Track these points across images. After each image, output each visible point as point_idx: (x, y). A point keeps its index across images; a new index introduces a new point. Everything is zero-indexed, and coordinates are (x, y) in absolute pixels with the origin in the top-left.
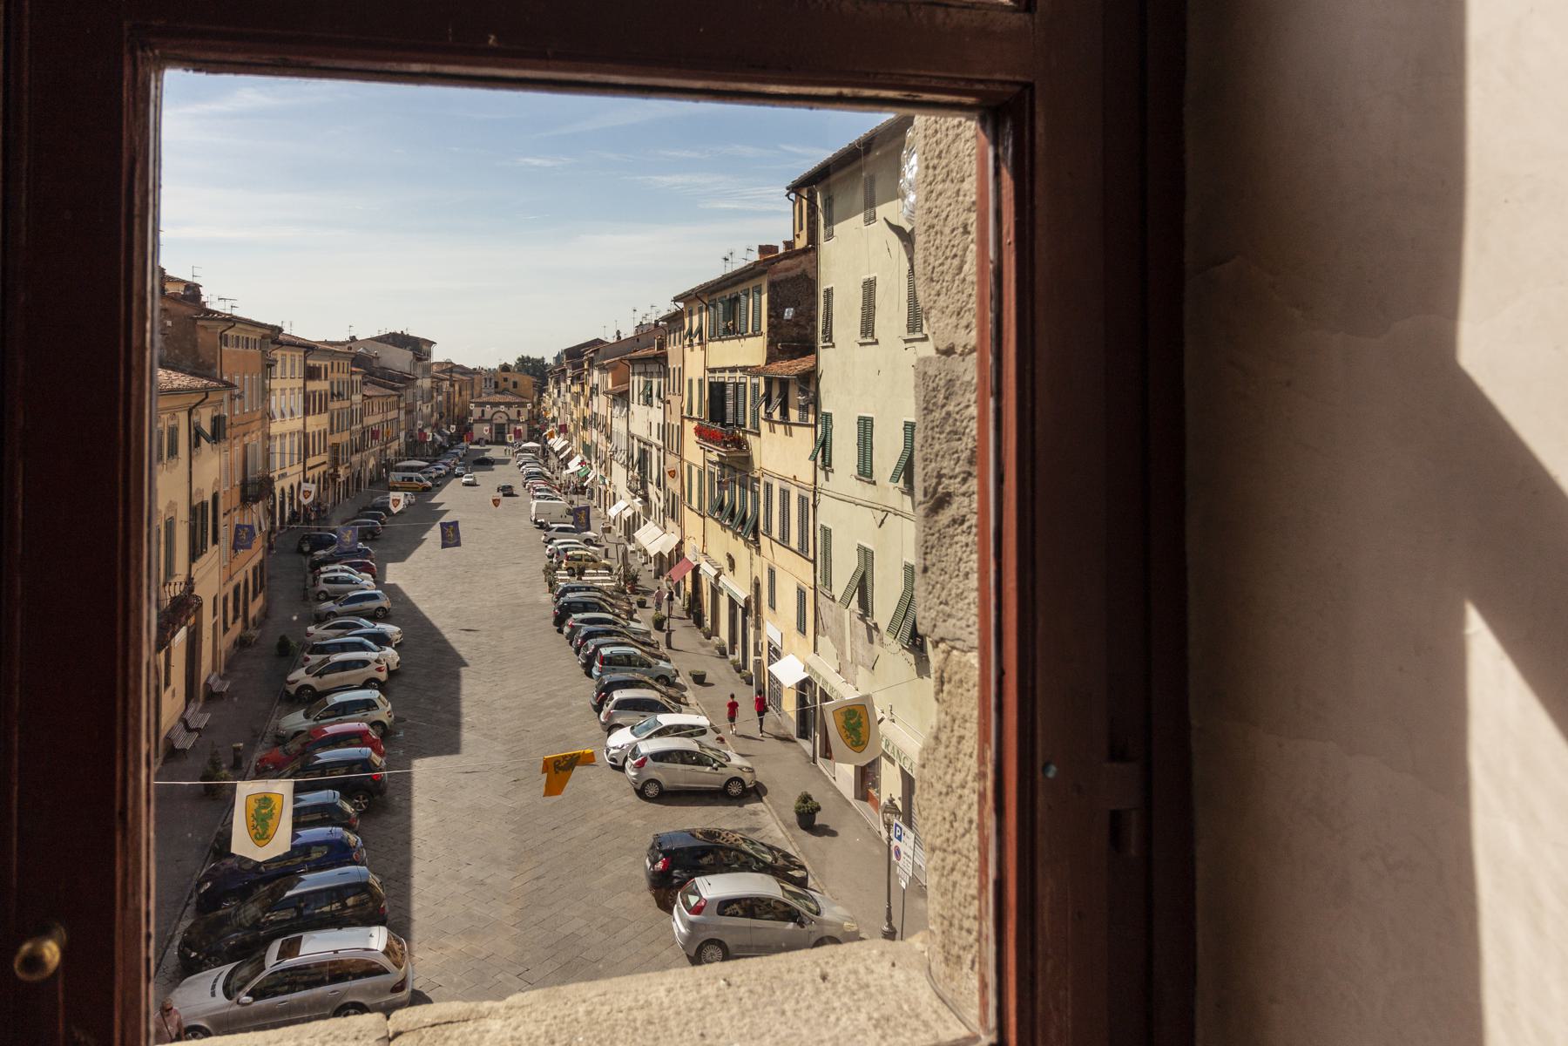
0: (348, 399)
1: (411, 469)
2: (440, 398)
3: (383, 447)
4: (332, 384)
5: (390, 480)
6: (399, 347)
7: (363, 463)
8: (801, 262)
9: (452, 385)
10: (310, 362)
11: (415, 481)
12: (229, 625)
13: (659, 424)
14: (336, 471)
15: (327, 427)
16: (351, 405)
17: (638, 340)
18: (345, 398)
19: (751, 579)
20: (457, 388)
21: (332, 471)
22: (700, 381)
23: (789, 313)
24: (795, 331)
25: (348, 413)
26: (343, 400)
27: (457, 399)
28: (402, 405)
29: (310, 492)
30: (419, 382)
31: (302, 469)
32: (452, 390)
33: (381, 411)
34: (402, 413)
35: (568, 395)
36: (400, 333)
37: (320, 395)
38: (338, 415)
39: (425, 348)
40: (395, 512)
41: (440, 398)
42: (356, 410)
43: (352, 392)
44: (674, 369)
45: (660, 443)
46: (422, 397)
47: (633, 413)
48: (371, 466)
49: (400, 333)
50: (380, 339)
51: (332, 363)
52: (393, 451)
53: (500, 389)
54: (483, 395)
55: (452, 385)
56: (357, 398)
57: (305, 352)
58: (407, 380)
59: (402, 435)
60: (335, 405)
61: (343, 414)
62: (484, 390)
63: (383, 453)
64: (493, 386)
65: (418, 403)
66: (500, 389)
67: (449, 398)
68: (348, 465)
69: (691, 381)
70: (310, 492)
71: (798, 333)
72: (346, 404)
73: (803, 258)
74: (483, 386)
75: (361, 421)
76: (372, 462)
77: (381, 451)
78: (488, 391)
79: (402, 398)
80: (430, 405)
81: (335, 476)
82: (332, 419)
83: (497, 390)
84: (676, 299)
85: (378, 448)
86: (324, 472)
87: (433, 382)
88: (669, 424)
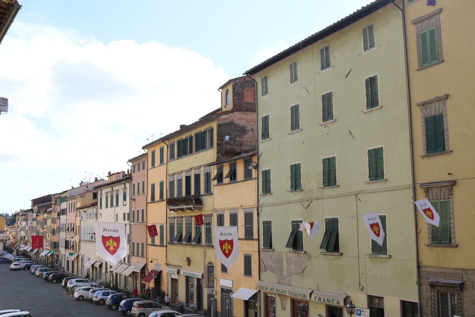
8: (231, 116)
13: (124, 214)
17: (87, 187)
19: (205, 264)
22: (162, 184)
23: (227, 138)
24: (228, 147)
35: (35, 224)
44: (139, 183)
45: (127, 222)
47: (101, 214)
69: (153, 186)
71: (230, 148)
73: (231, 114)
84: (144, 148)
88: (134, 211)
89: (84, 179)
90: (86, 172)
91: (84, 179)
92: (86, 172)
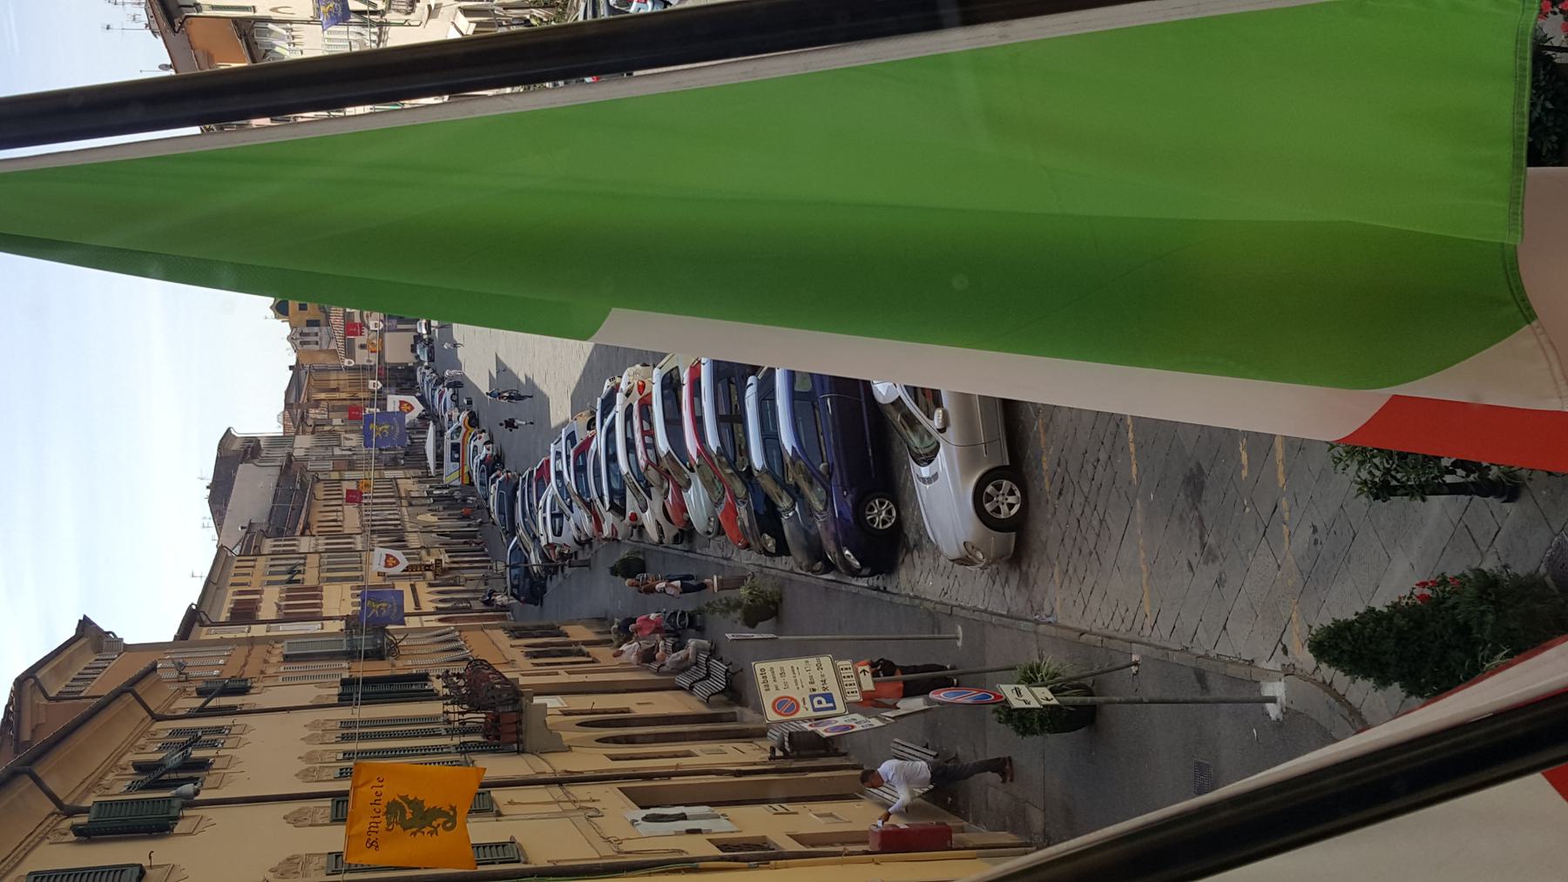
0: (305, 558)
1: (439, 457)
2: (337, 421)
3: (404, 503)
4: (270, 583)
5: (458, 483)
6: (231, 489)
7: (426, 529)
9: (317, 403)
10: (224, 615)
11: (459, 440)
12: (590, 659)
14: (428, 568)
15: (347, 586)
16: (316, 552)
18: (302, 561)
20: (323, 396)
21: (429, 574)
25: (329, 557)
26: (304, 564)
27: (344, 396)
28: (335, 476)
29: (388, 556)
30: (298, 453)
31: (417, 618)
32: (324, 404)
33: (340, 508)
34: (348, 475)
36: (209, 491)
37: (288, 598)
38: (329, 570)
39: (236, 446)
40: (422, 408)
41: (337, 421)
42: (327, 544)
43: (293, 552)
46: (327, 447)
48: (435, 519)
49: (209, 491)
50: (219, 525)
51: (232, 585)
52: (416, 487)
53: (322, 317)
54: (333, 347)
55: (317, 403)
56: (305, 544)
57: (202, 625)
58: (289, 468)
59: (389, 474)
60: (310, 577)
61: (329, 563)
62: (325, 347)
63: (414, 502)
64: (316, 329)
65: (337, 451)
66: (322, 317)
67: (340, 409)
68: (423, 552)
70: (388, 556)
72: (313, 560)
74: (317, 348)
75: (350, 536)
76: (429, 518)
77: (411, 505)
78: (326, 338)
79: (321, 477)
80: (344, 435)
81: (438, 569)
82: (330, 580)
83: (322, 322)
85: (404, 509)
86: (431, 585)
87: (304, 433)
89: (134, 19)
90: (108, 28)
91: (134, 19)
92: (108, 28)
